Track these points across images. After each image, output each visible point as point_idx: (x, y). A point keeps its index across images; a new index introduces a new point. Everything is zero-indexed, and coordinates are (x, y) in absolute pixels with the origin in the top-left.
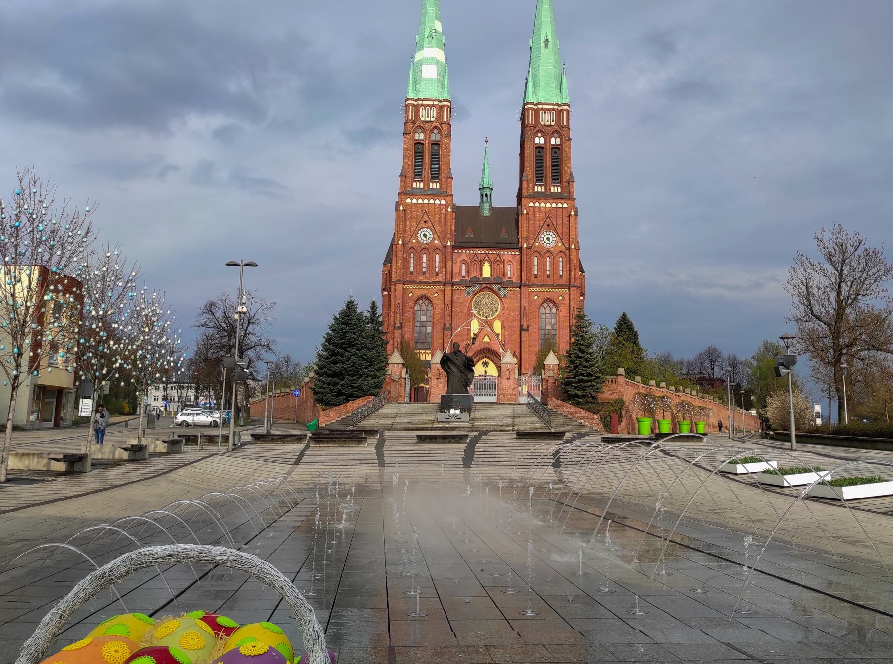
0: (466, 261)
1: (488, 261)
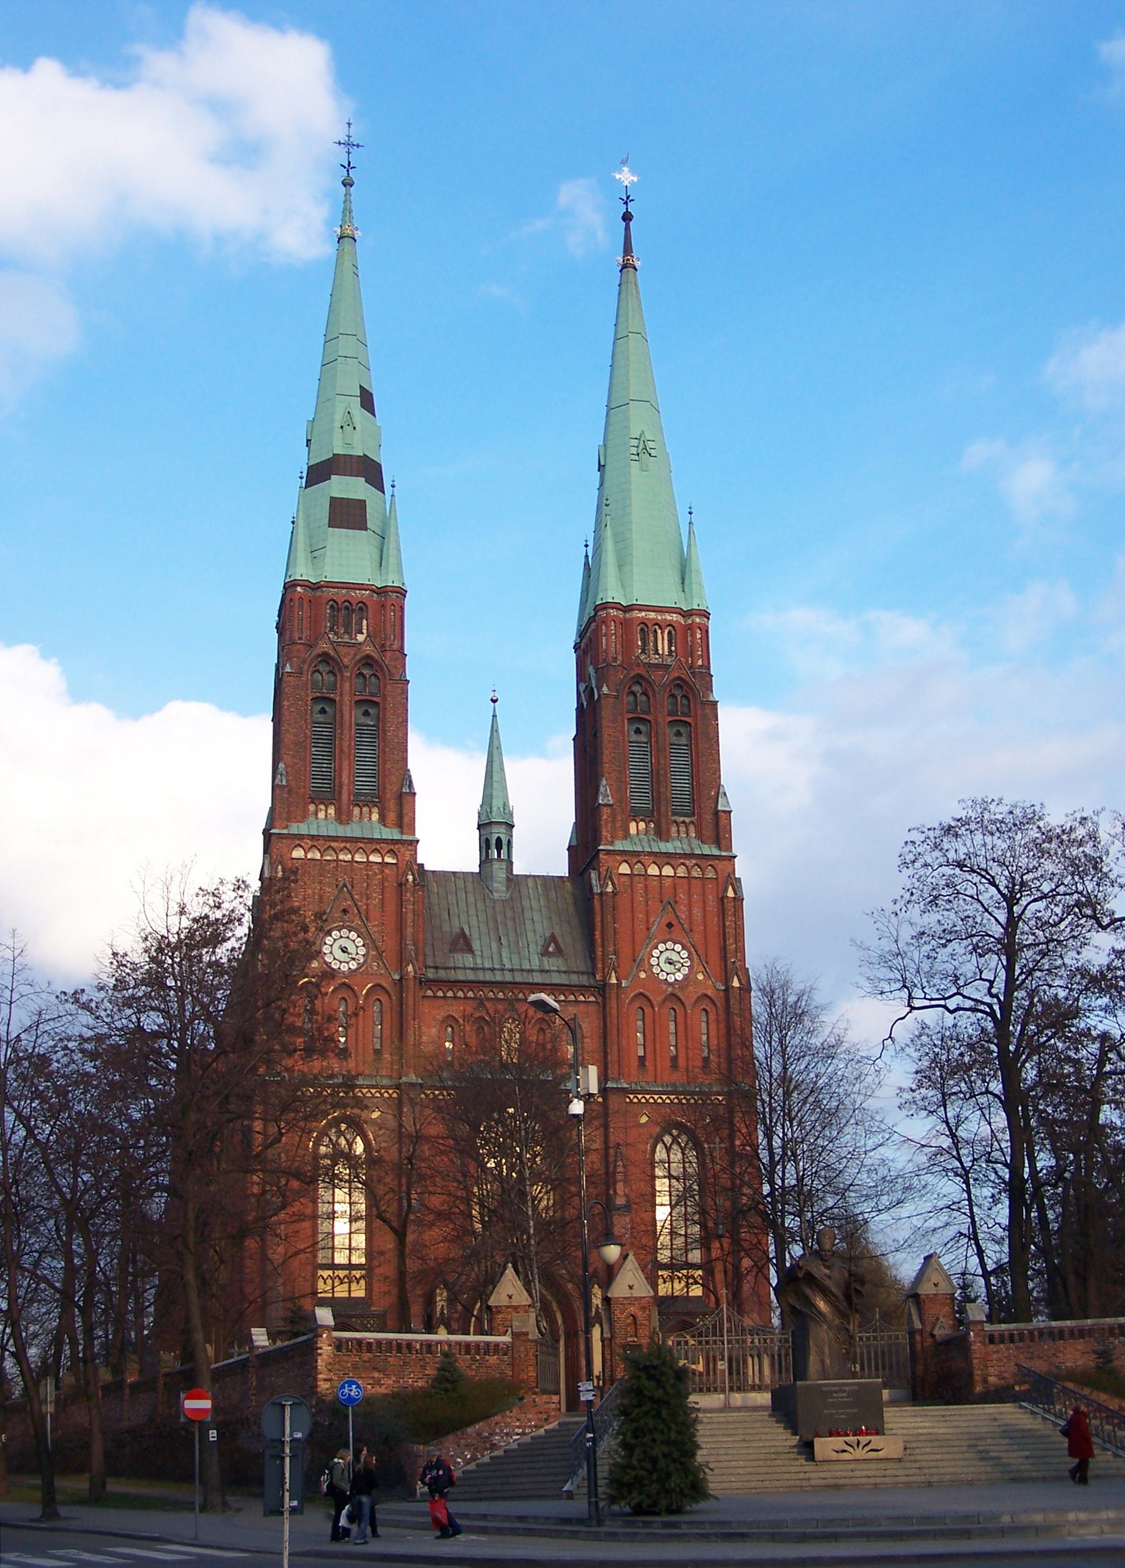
0: (457, 1021)
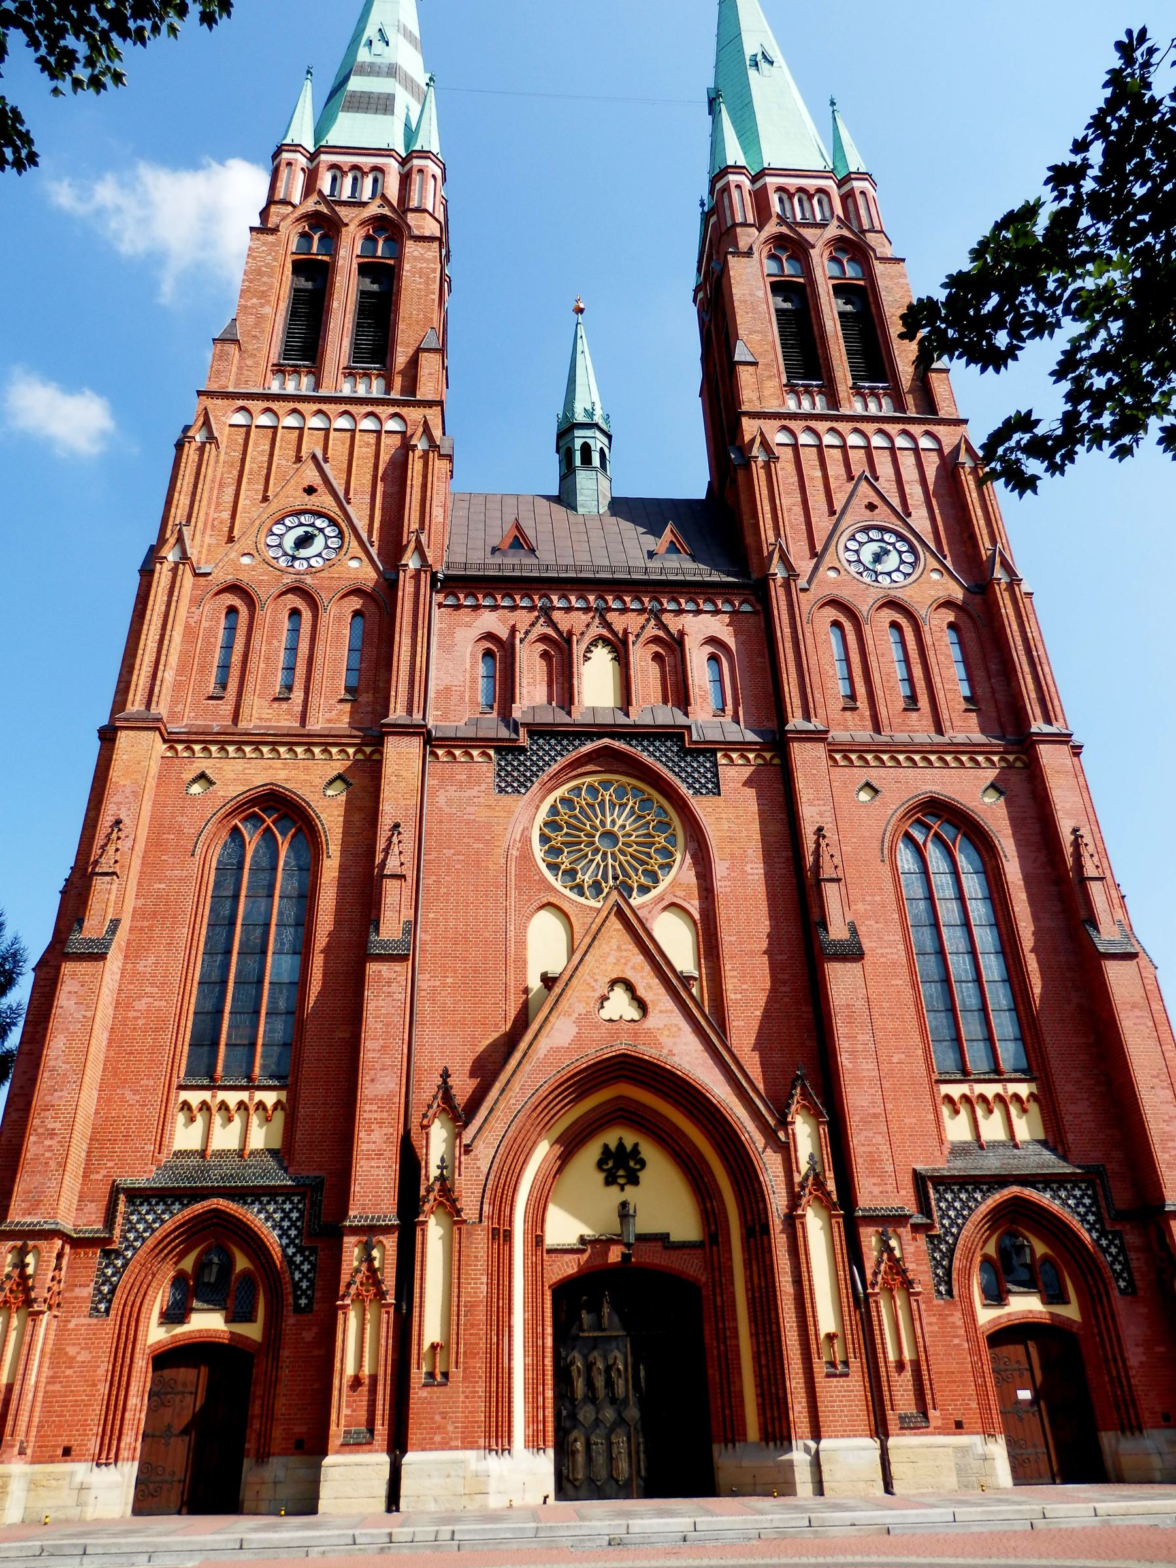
1: (606, 642)
